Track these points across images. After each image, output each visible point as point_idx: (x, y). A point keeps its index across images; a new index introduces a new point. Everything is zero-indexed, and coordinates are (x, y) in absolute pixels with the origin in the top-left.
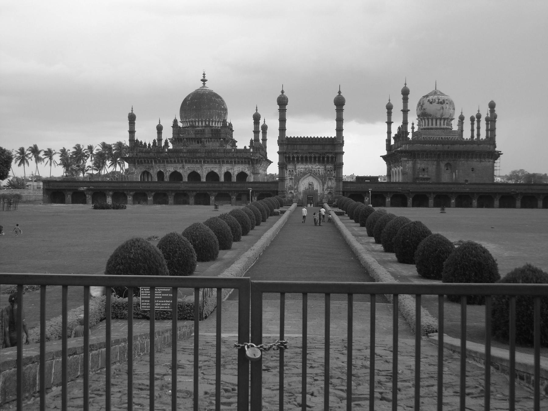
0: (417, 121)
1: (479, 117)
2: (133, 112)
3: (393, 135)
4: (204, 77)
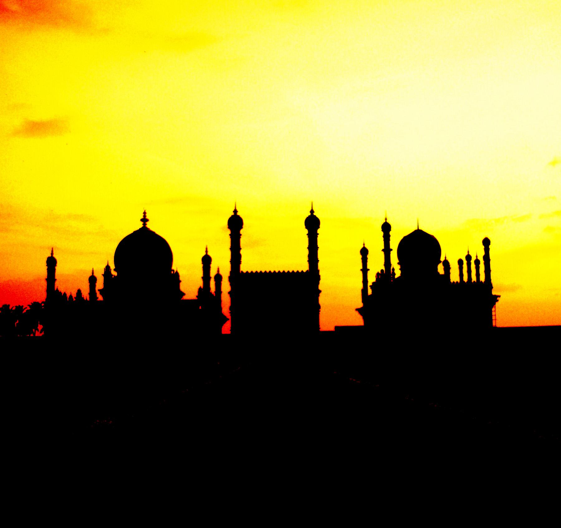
0: (399, 267)
1: (469, 257)
2: (54, 256)
3: (370, 284)
4: (145, 216)
